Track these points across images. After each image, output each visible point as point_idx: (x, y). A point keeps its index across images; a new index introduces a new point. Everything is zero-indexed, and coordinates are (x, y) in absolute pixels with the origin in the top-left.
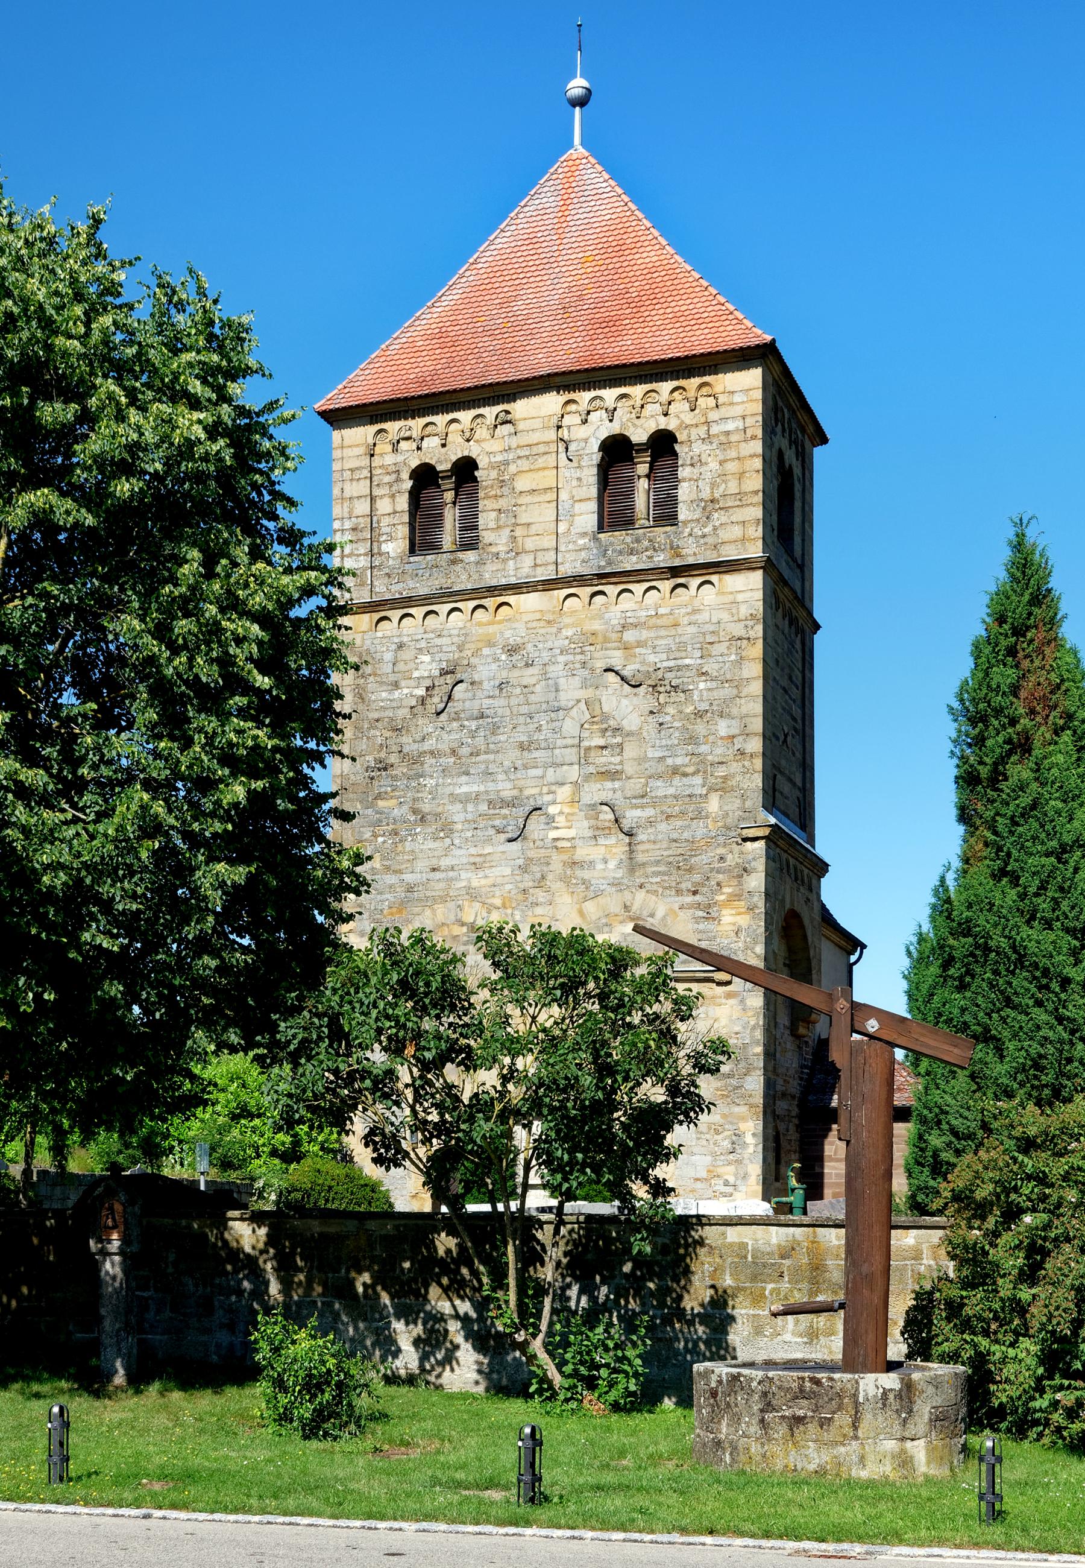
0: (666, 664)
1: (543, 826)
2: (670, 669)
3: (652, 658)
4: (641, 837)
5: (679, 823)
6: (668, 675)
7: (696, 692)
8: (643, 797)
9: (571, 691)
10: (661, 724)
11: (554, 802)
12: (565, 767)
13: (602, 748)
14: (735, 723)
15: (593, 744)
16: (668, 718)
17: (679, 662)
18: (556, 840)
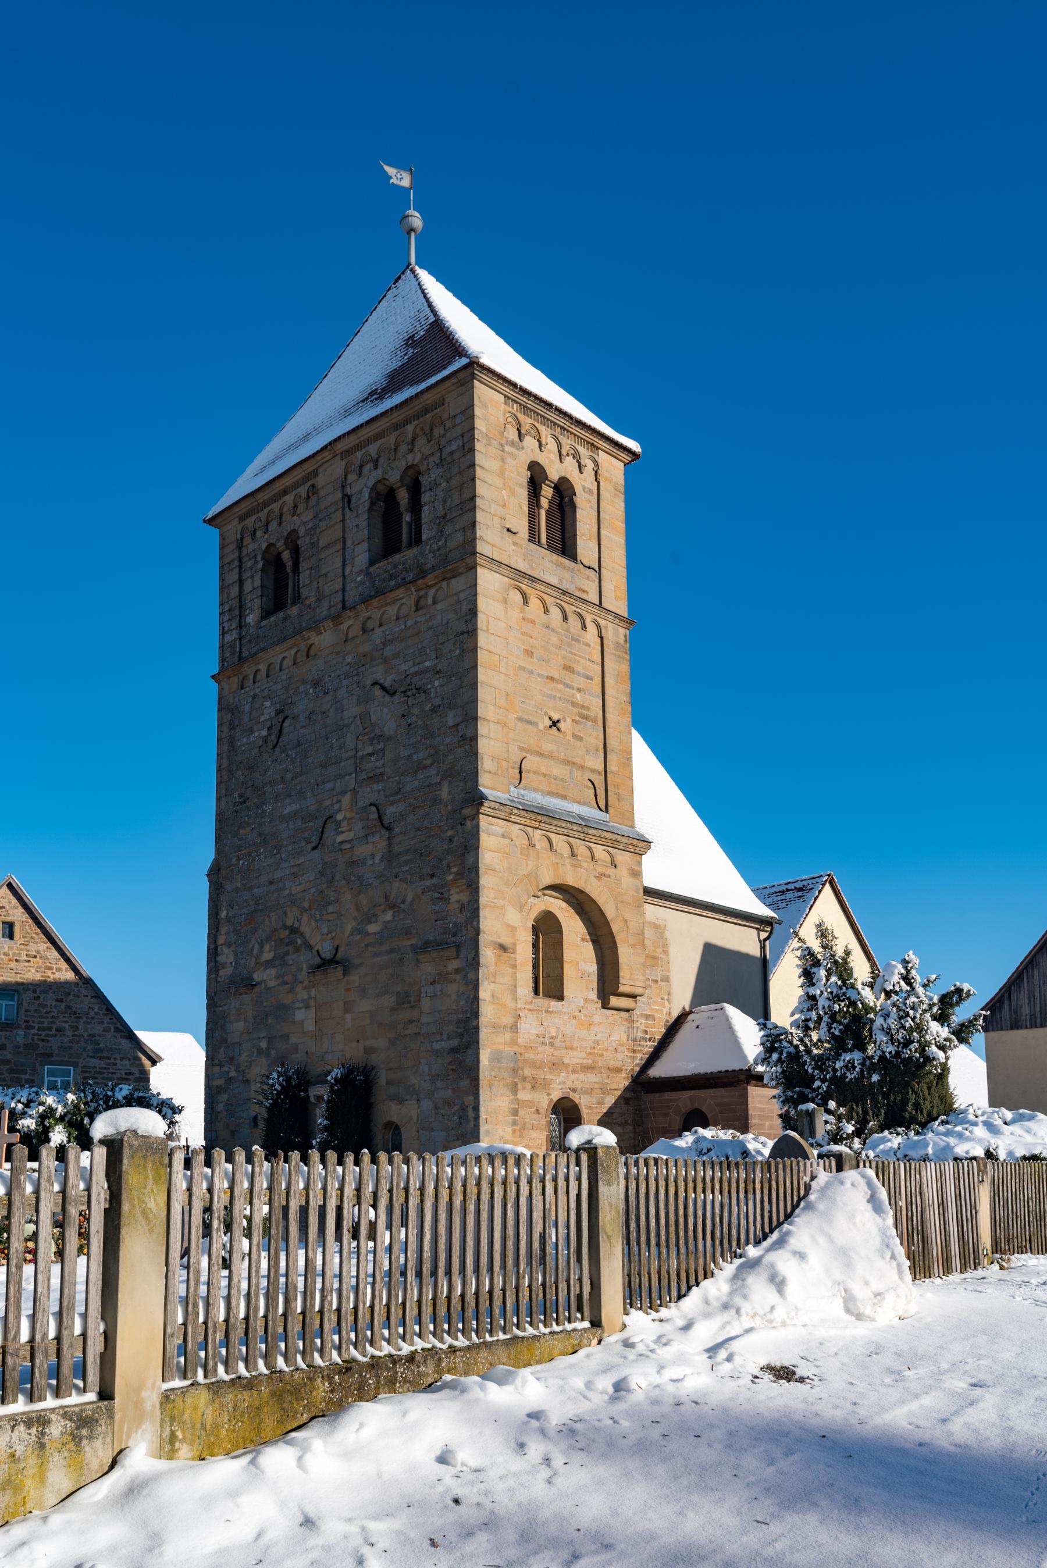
0: (413, 670)
1: (333, 833)
2: (415, 674)
3: (403, 667)
4: (397, 830)
5: (421, 813)
6: (415, 679)
7: (432, 690)
8: (397, 793)
9: (352, 710)
10: (409, 725)
11: (340, 810)
12: (347, 777)
15: (365, 753)
16: (414, 718)
18: (341, 843)
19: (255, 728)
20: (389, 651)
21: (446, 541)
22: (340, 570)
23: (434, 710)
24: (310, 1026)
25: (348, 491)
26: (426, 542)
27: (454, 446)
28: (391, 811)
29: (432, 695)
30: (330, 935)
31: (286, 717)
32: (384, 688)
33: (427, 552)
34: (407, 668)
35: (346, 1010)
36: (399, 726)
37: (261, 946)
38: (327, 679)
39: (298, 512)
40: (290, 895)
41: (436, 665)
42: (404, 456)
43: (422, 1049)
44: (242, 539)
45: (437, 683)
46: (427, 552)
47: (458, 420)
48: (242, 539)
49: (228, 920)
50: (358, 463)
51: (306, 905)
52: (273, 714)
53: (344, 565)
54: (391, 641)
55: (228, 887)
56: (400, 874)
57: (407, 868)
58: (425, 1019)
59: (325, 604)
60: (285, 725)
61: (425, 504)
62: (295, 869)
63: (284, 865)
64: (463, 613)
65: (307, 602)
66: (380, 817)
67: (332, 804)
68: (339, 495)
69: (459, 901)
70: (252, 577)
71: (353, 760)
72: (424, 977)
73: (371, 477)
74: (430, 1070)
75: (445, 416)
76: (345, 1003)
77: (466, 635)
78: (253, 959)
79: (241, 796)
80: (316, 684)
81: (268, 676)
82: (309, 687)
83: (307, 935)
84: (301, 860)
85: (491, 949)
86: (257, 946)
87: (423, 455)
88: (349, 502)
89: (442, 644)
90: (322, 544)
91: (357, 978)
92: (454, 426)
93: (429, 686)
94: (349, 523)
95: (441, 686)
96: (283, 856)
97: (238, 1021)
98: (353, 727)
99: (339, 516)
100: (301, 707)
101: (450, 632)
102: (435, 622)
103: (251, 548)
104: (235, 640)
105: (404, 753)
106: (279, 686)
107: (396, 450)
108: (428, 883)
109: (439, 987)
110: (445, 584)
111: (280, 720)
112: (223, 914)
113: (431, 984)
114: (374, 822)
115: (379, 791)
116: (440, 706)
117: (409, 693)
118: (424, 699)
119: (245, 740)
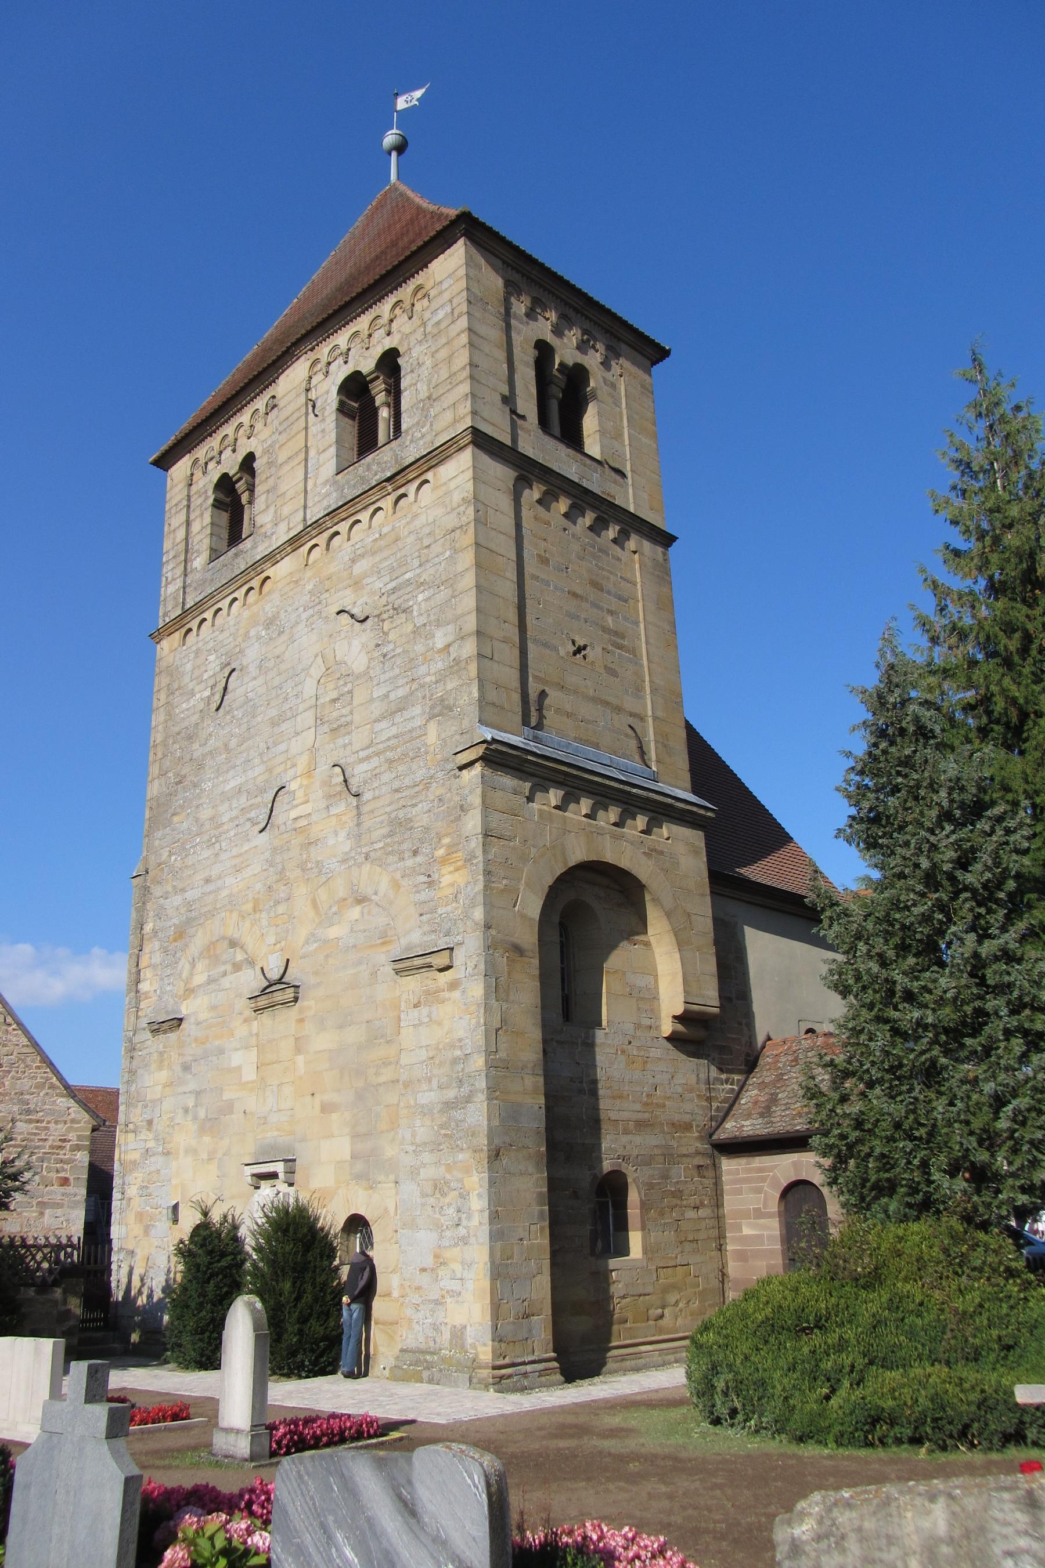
2: (394, 590)
4: (367, 796)
6: (393, 597)
7: (415, 607)
10: (385, 656)
13: (334, 701)
14: (450, 628)
16: (391, 646)
17: (400, 580)
19: (197, 689)
20: (360, 568)
21: (431, 425)
22: (302, 485)
23: (416, 631)
24: (249, 1074)
25: (313, 395)
26: (407, 431)
27: (441, 314)
28: (359, 773)
29: (415, 613)
30: (278, 945)
31: (233, 670)
32: (352, 616)
33: (408, 443)
34: (381, 586)
35: (298, 1050)
36: (371, 659)
37: (193, 964)
38: (282, 615)
39: (256, 431)
40: (230, 895)
41: (419, 575)
42: (379, 342)
43: (402, 1104)
44: (192, 475)
45: (420, 597)
46: (408, 443)
47: (445, 286)
48: (192, 475)
49: (155, 932)
50: (324, 360)
51: (249, 907)
52: (218, 669)
53: (306, 479)
54: (362, 556)
55: (157, 891)
56: (372, 854)
57: (381, 845)
58: (405, 1060)
59: (283, 527)
60: (231, 679)
61: (406, 389)
62: (238, 861)
63: (223, 856)
64: (455, 505)
65: (263, 530)
66: (345, 781)
67: (286, 770)
68: (302, 399)
69: (452, 885)
70: (202, 515)
71: (313, 710)
72: (405, 997)
73: (340, 373)
74: (414, 1136)
75: (428, 286)
76: (297, 1039)
77: (458, 531)
78: (182, 984)
79: (177, 775)
80: (269, 623)
81: (213, 625)
82: (260, 628)
83: (250, 948)
84: (246, 848)
85: (501, 951)
86: (187, 966)
87: (404, 334)
88: (314, 407)
89: (428, 547)
90: (282, 458)
91: (312, 1003)
92: (441, 293)
93: (411, 603)
94: (313, 430)
95: (426, 600)
96: (223, 844)
97: (160, 1068)
98: (312, 671)
99: (302, 423)
100: (253, 654)
101: (437, 531)
102: (417, 523)
103: (201, 484)
104: (178, 589)
105: (378, 692)
106: (226, 634)
107: (370, 335)
108: (410, 863)
109: (424, 1010)
110: (429, 476)
111: (226, 675)
112: (148, 927)
113: (415, 1006)
114: (338, 789)
115: (345, 746)
116: (425, 625)
117: (385, 616)
118: (404, 620)
119: (184, 705)
